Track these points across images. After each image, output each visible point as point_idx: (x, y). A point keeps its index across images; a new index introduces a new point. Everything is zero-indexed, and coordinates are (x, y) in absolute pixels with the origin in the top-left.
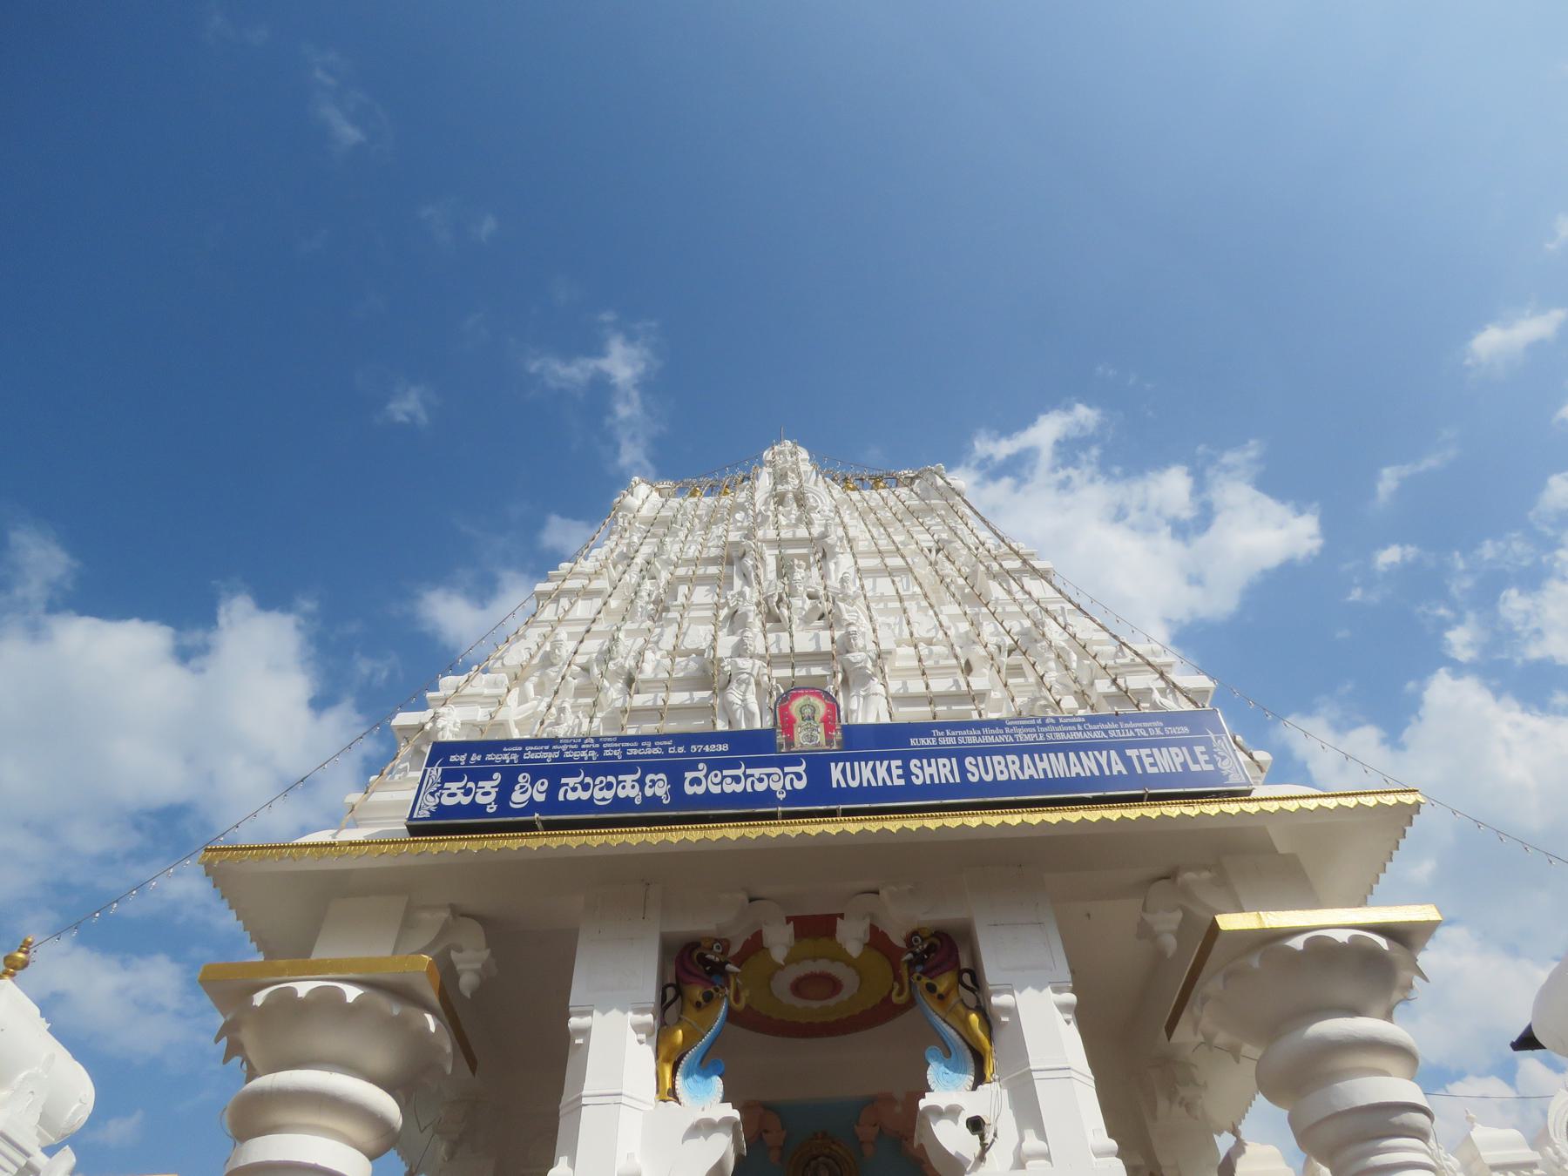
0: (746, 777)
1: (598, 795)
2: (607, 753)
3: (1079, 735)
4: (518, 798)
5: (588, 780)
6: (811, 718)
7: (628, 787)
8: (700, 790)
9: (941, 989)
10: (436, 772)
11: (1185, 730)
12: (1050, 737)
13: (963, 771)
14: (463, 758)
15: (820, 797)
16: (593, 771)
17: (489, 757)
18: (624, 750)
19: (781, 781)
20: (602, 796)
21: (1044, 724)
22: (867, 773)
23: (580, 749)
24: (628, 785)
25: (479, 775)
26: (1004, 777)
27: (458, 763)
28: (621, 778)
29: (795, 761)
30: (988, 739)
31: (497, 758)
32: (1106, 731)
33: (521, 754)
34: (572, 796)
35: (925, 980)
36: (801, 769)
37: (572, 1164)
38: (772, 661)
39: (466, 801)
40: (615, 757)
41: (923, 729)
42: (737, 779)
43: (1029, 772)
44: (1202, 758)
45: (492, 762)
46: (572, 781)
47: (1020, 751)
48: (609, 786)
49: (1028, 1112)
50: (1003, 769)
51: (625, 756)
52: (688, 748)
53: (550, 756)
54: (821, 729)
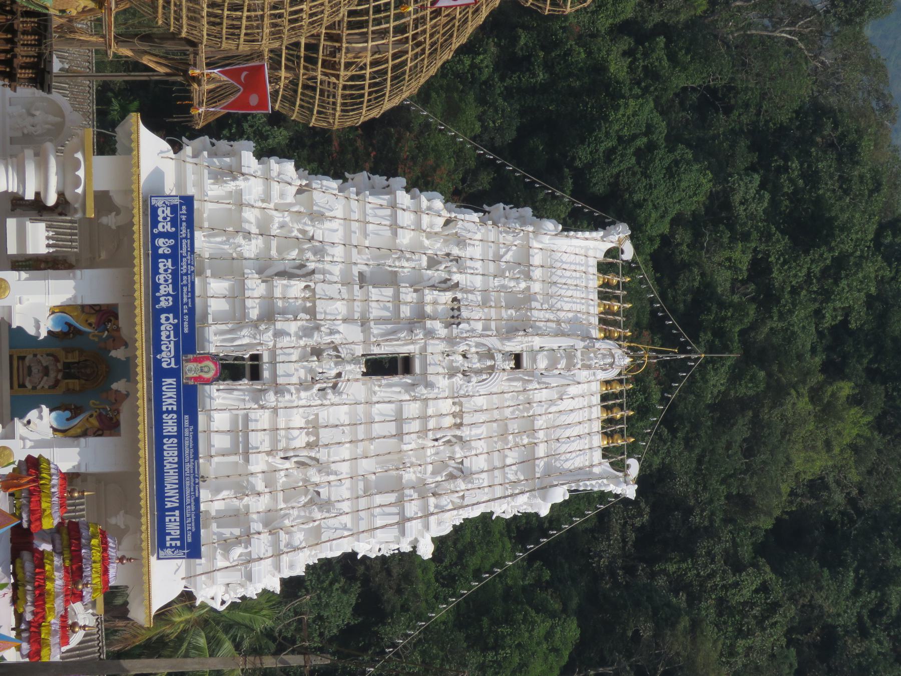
0: (169, 342)
1: (161, 277)
2: (185, 278)
3: (188, 492)
4: (160, 242)
5: (170, 271)
6: (202, 371)
7: (165, 289)
8: (163, 321)
9: (91, 419)
10: (177, 201)
11: (190, 540)
12: (187, 479)
13: (170, 437)
14: (184, 212)
15: (159, 373)
16: (175, 274)
17: (184, 224)
18: (187, 285)
19: (167, 358)
20: (161, 279)
21: (195, 477)
22: (170, 395)
23: (187, 265)
24: (167, 289)
25: (174, 222)
26: (165, 453)
27: (181, 210)
28: (171, 286)
29: (177, 362)
31: (184, 228)
32: (190, 504)
33: (186, 238)
34: (161, 265)
35: (95, 414)
36: (173, 365)
37: (26, 279)
38: (273, 353)
39: (160, 219)
40: (182, 281)
41: (194, 422)
42: (168, 337)
43: (168, 466)
44: (173, 543)
45: (181, 226)
46: (169, 263)
47: (180, 463)
48: (166, 281)
50: (170, 455)
51: (182, 286)
52: (186, 314)
53: (184, 252)
54: (195, 375)
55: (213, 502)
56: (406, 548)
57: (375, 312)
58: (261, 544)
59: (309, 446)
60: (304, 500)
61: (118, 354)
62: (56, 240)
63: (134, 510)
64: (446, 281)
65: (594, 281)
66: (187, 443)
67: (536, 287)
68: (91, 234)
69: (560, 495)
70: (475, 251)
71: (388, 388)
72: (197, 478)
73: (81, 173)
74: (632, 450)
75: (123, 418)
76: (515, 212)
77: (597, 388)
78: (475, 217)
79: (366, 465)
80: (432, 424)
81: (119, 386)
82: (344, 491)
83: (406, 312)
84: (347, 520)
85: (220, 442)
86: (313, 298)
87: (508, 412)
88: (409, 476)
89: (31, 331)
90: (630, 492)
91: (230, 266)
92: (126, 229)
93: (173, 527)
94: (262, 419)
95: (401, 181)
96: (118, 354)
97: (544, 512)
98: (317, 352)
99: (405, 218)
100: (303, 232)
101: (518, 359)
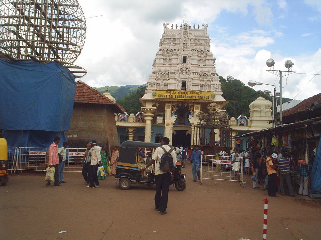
60: (207, 75)
62: (160, 115)
64: (171, 52)
73: (149, 109)
81: (186, 105)
89: (175, 120)
100: (161, 73)
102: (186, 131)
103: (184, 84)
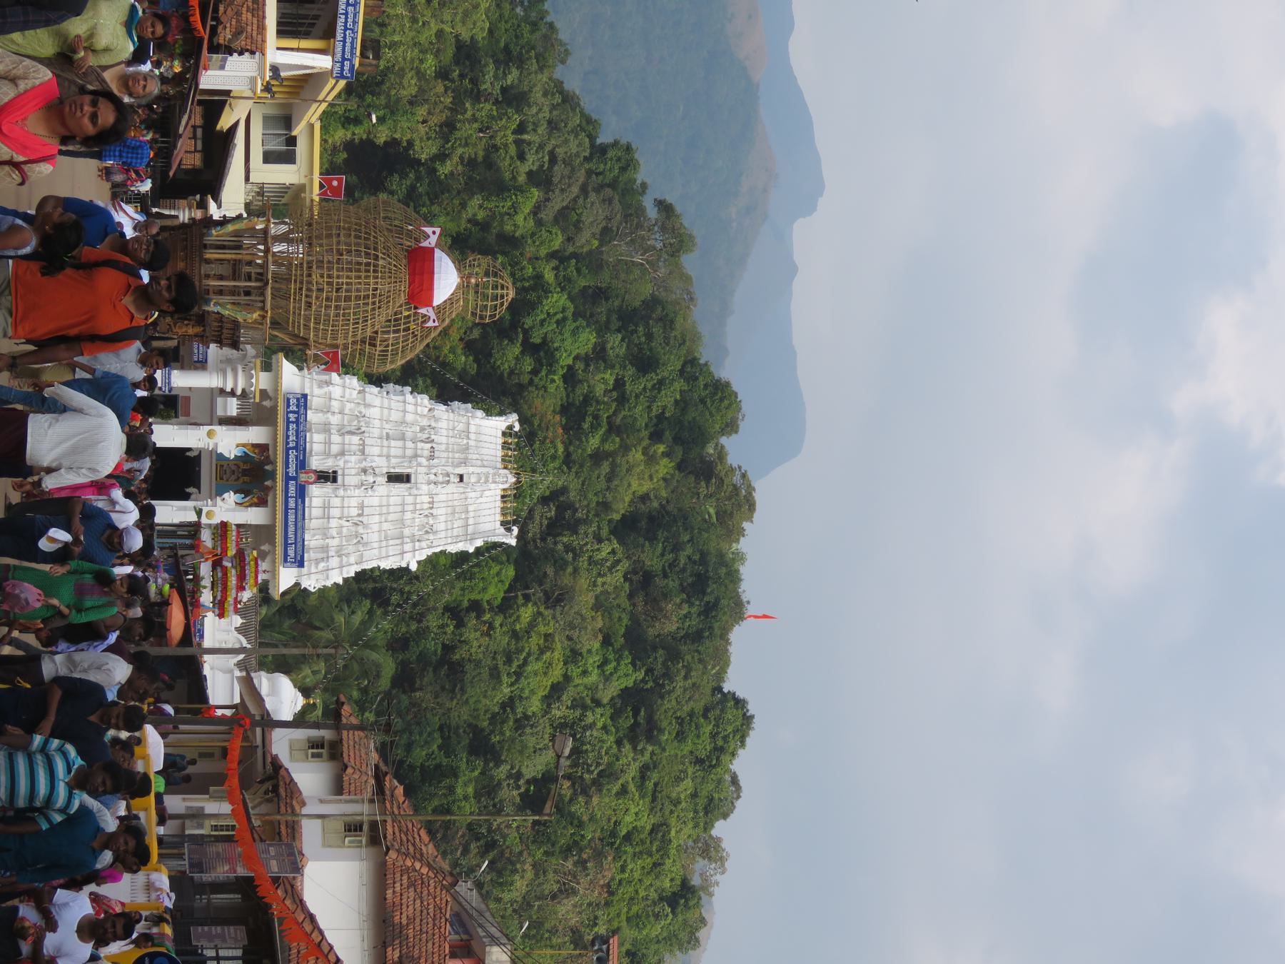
15: (288, 478)
19: (292, 471)
25: (298, 406)
30: (300, 516)
41: (303, 502)
49: (228, 510)
50: (291, 518)
55: (311, 540)
56: (404, 565)
57: (393, 452)
58: (334, 562)
59: (359, 515)
61: (268, 468)
63: (273, 544)
65: (500, 440)
66: (300, 513)
67: (472, 443)
68: (257, 411)
69: (479, 543)
70: (443, 424)
71: (400, 488)
72: (303, 528)
73: (253, 381)
74: (515, 522)
75: (270, 499)
76: (463, 406)
77: (500, 493)
78: (444, 408)
79: (385, 526)
80: (418, 507)
81: (268, 483)
82: (375, 537)
83: (409, 453)
84: (376, 551)
85: (316, 512)
86: (364, 445)
87: (456, 503)
88: (407, 532)
90: (513, 542)
91: (326, 428)
92: (274, 409)
93: (291, 552)
94: (336, 502)
95: (409, 389)
96: (268, 468)
97: (471, 550)
98: (365, 471)
99: (410, 408)
101: (461, 478)
102: (199, 488)
103: (328, 477)
